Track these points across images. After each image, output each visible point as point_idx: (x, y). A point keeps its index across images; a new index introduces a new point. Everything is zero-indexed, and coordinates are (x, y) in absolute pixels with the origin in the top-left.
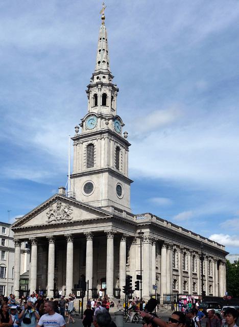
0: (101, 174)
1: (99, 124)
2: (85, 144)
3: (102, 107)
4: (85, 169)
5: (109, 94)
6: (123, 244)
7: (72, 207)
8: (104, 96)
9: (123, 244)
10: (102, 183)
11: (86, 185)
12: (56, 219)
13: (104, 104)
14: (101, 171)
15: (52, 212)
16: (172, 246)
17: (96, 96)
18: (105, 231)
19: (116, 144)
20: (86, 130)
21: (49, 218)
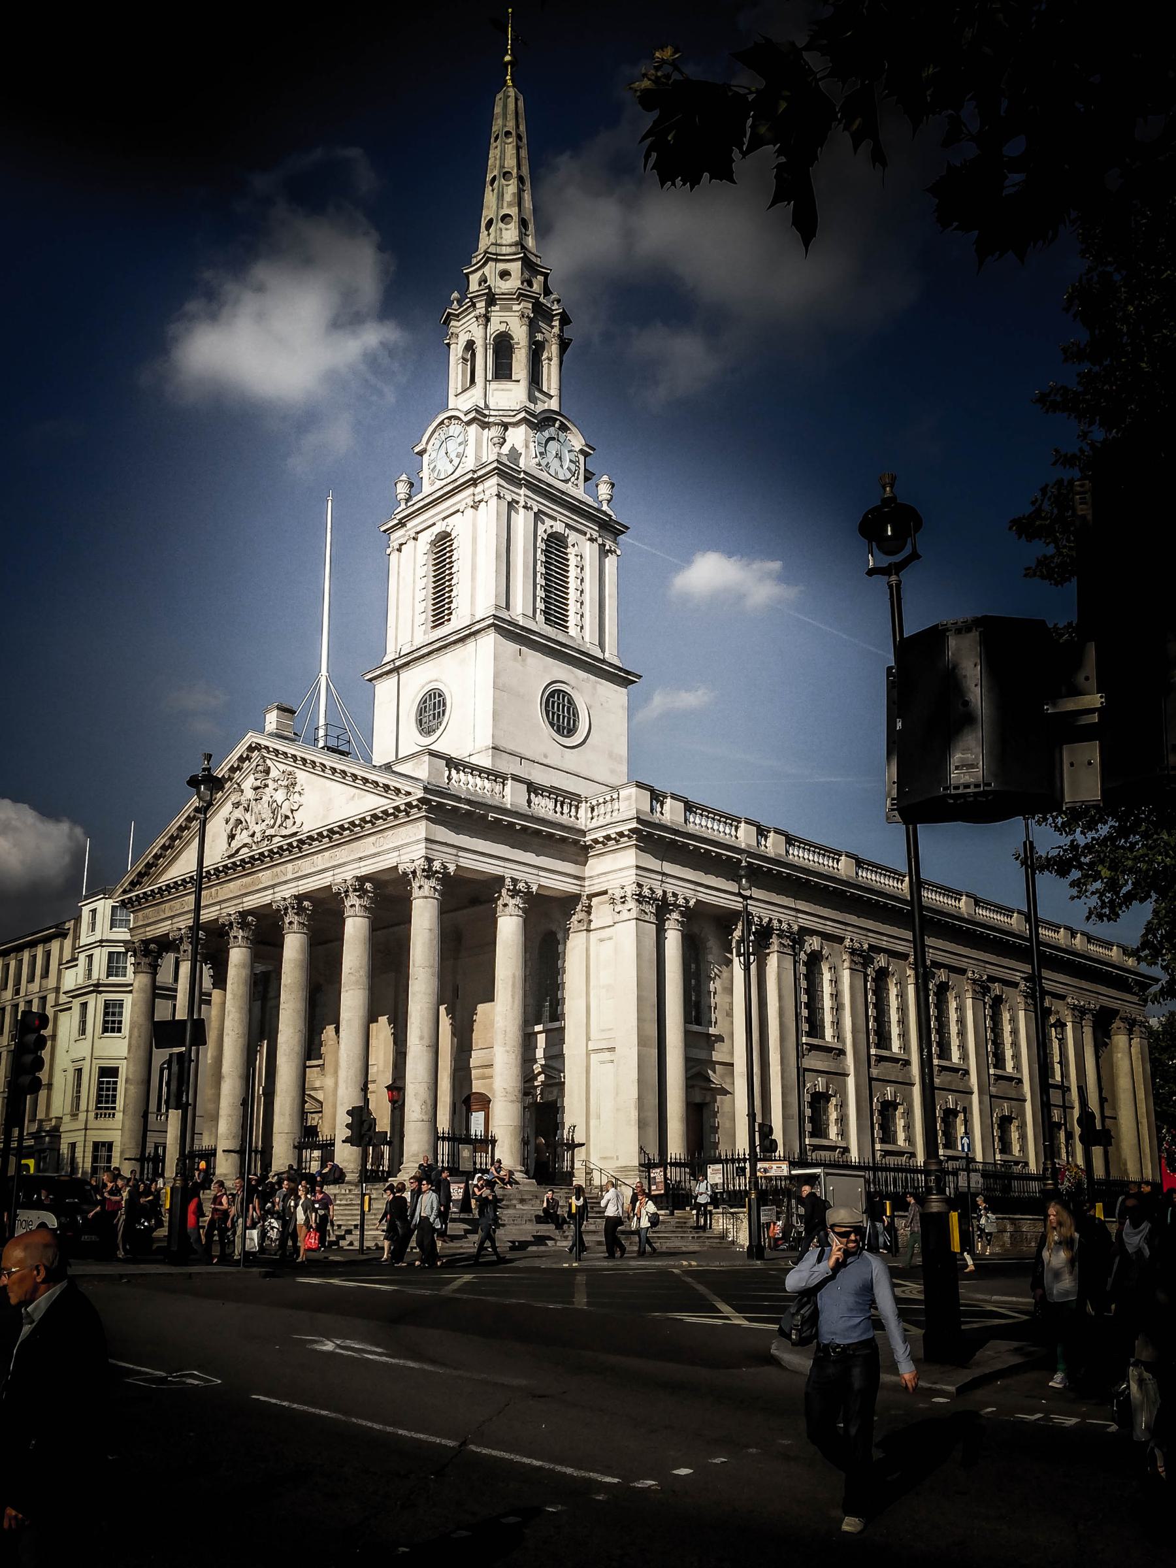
0: (471, 645)
1: (470, 451)
2: (427, 537)
3: (494, 386)
4: (423, 636)
5: (520, 333)
6: (509, 927)
7: (302, 776)
8: (503, 346)
9: (509, 927)
10: (473, 680)
11: (424, 701)
12: (249, 840)
13: (502, 371)
14: (468, 635)
15: (238, 813)
16: (797, 939)
17: (470, 346)
18: (401, 869)
19: (549, 522)
20: (433, 484)
21: (232, 837)
